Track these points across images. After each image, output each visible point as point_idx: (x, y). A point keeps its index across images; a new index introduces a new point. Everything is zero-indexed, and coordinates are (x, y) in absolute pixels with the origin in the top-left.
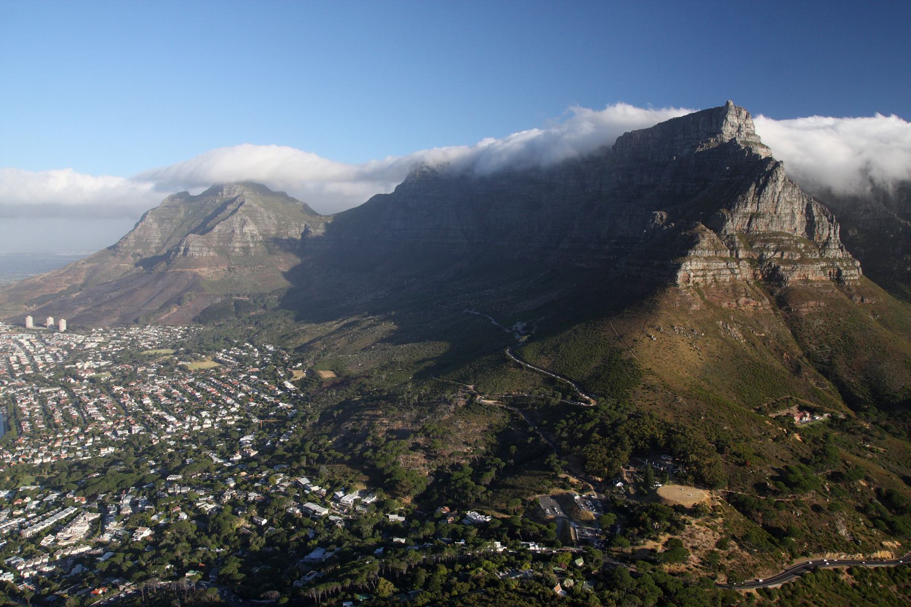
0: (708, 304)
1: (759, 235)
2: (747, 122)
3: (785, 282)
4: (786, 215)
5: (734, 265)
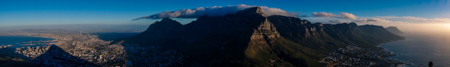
0: (256, 43)
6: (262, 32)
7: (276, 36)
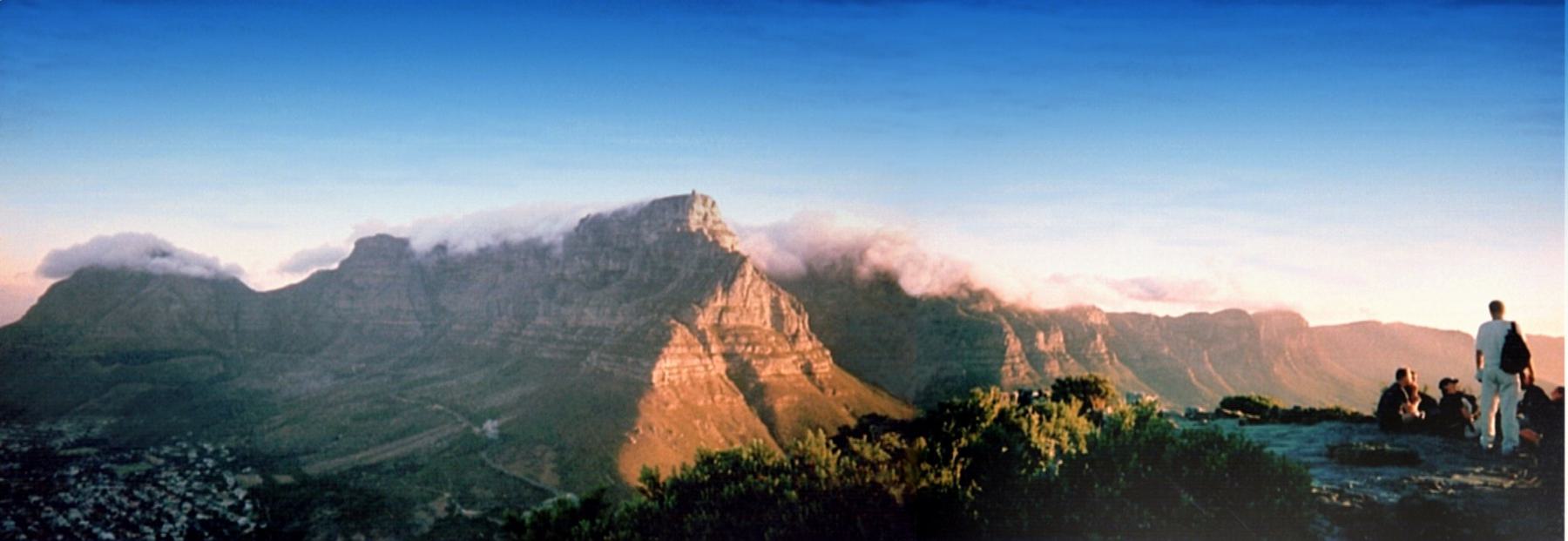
3: (756, 376)
5: (708, 361)
6: (722, 338)
7: (808, 371)
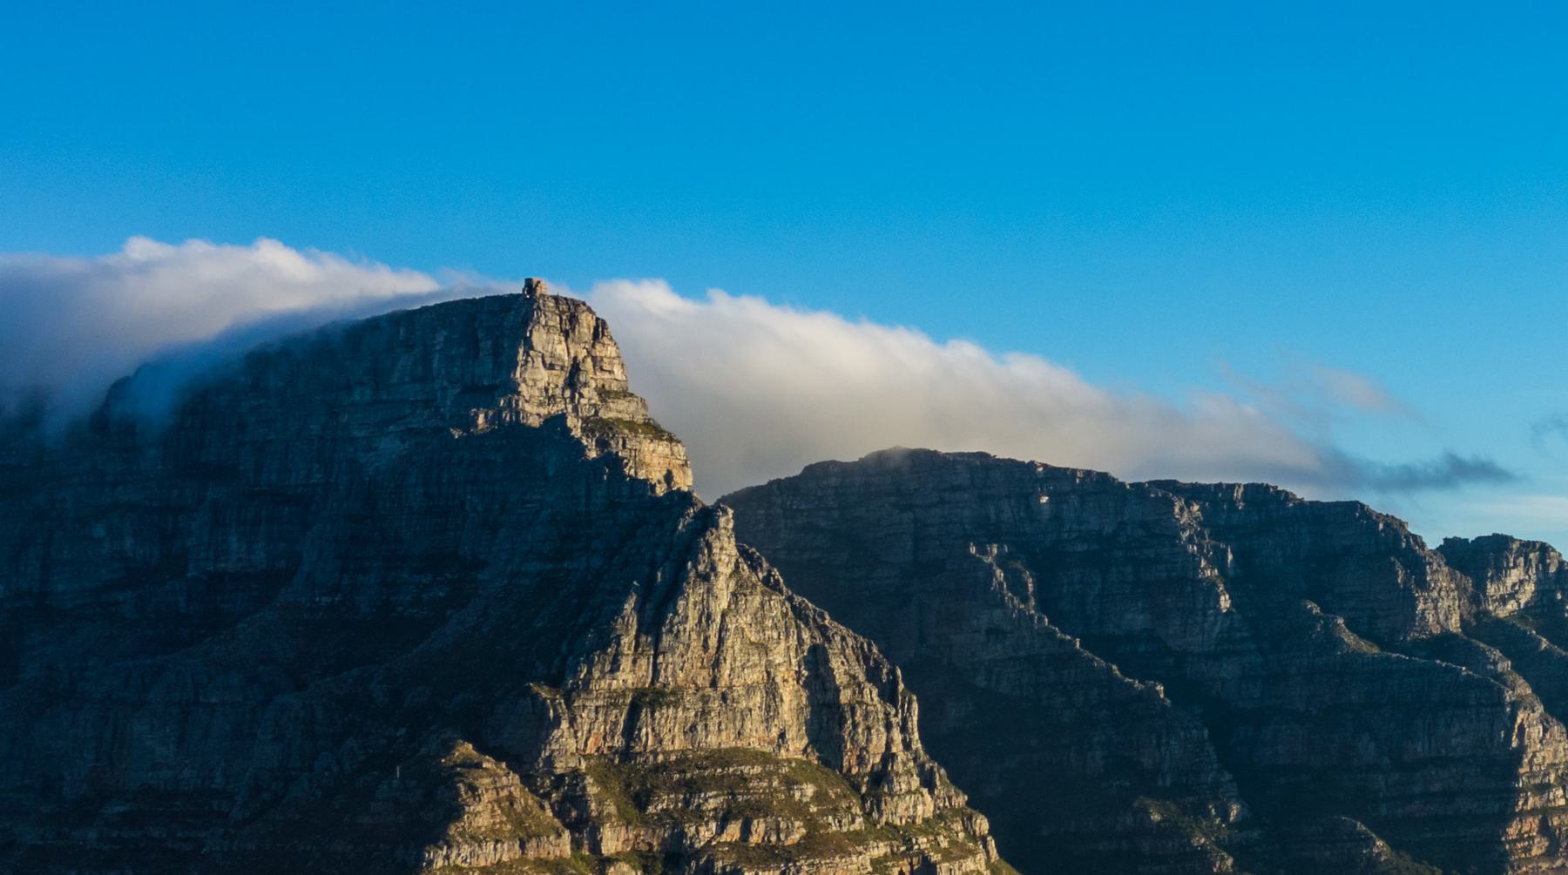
1: (664, 767)
2: (599, 351)
4: (750, 689)
